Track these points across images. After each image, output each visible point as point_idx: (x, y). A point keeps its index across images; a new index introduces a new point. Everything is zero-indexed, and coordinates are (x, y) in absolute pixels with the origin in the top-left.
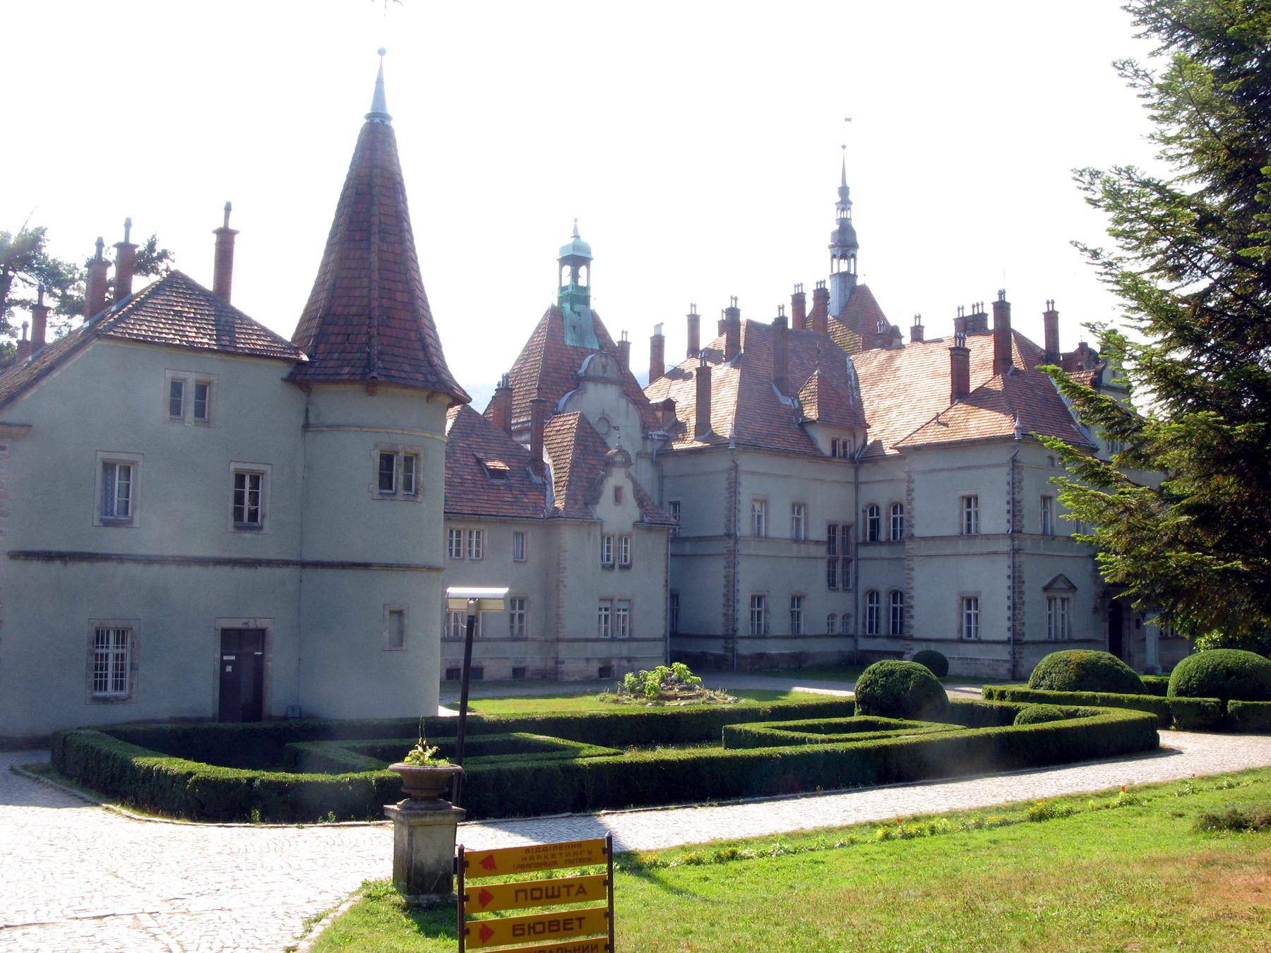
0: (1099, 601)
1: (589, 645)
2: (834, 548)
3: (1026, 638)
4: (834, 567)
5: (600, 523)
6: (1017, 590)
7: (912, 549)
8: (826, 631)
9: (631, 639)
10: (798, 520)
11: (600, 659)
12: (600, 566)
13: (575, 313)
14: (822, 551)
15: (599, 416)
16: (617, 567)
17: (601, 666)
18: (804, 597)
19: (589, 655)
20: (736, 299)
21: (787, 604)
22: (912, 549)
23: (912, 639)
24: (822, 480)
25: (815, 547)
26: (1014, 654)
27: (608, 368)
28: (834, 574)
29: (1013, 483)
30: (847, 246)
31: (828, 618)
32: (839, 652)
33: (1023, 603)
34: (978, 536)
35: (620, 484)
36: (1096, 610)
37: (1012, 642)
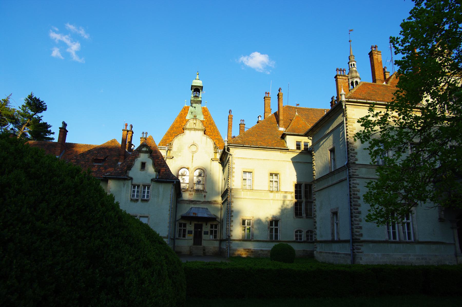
0: (443, 213)
3: (365, 238)
5: (131, 179)
8: (294, 239)
12: (130, 200)
13: (193, 107)
16: (140, 200)
18: (279, 221)
20: (268, 93)
23: (316, 241)
26: (353, 249)
27: (197, 124)
29: (347, 132)
30: (353, 78)
31: (296, 232)
32: (304, 250)
35: (144, 161)
36: (441, 220)
37: (351, 241)
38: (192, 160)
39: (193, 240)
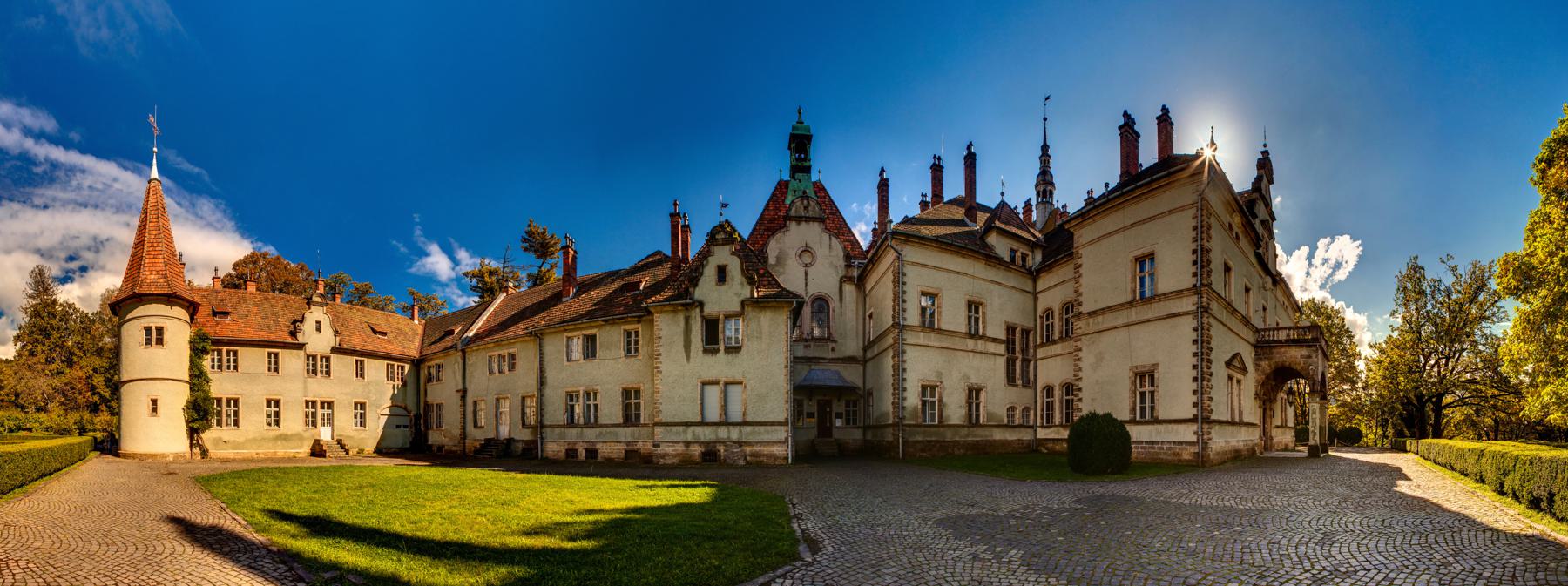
1: (692, 428)
2: (1014, 349)
3: (1214, 417)
4: (1014, 365)
6: (1205, 357)
7: (1080, 328)
9: (745, 423)
10: (977, 320)
11: (701, 444)
14: (1001, 349)
15: (804, 249)
17: (703, 450)
19: (689, 438)
21: (963, 396)
22: (1080, 328)
24: (999, 284)
25: (993, 344)
28: (1014, 370)
33: (1211, 375)
34: (1154, 298)
38: (806, 279)
39: (816, 430)
